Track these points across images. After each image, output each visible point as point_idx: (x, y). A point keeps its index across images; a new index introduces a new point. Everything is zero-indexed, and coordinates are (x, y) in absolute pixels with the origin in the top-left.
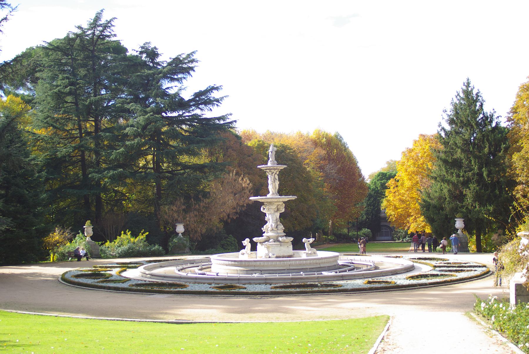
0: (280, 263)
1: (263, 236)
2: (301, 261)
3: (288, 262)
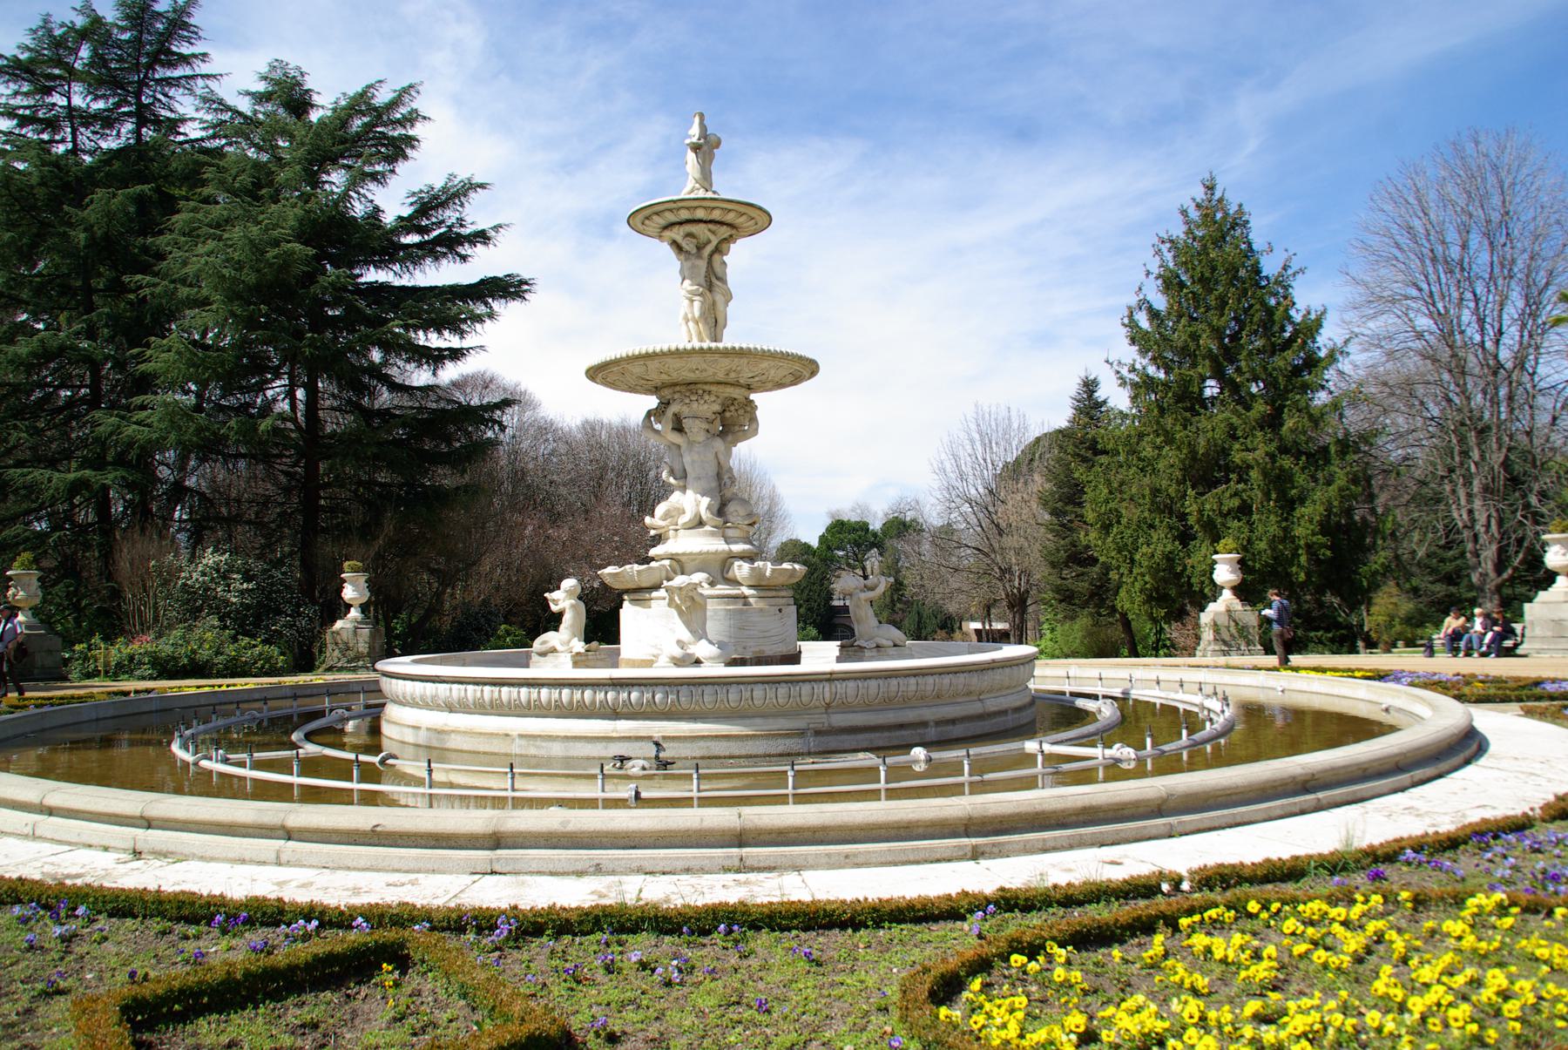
0: (771, 694)
1: (647, 560)
2: (894, 682)
3: (818, 688)
